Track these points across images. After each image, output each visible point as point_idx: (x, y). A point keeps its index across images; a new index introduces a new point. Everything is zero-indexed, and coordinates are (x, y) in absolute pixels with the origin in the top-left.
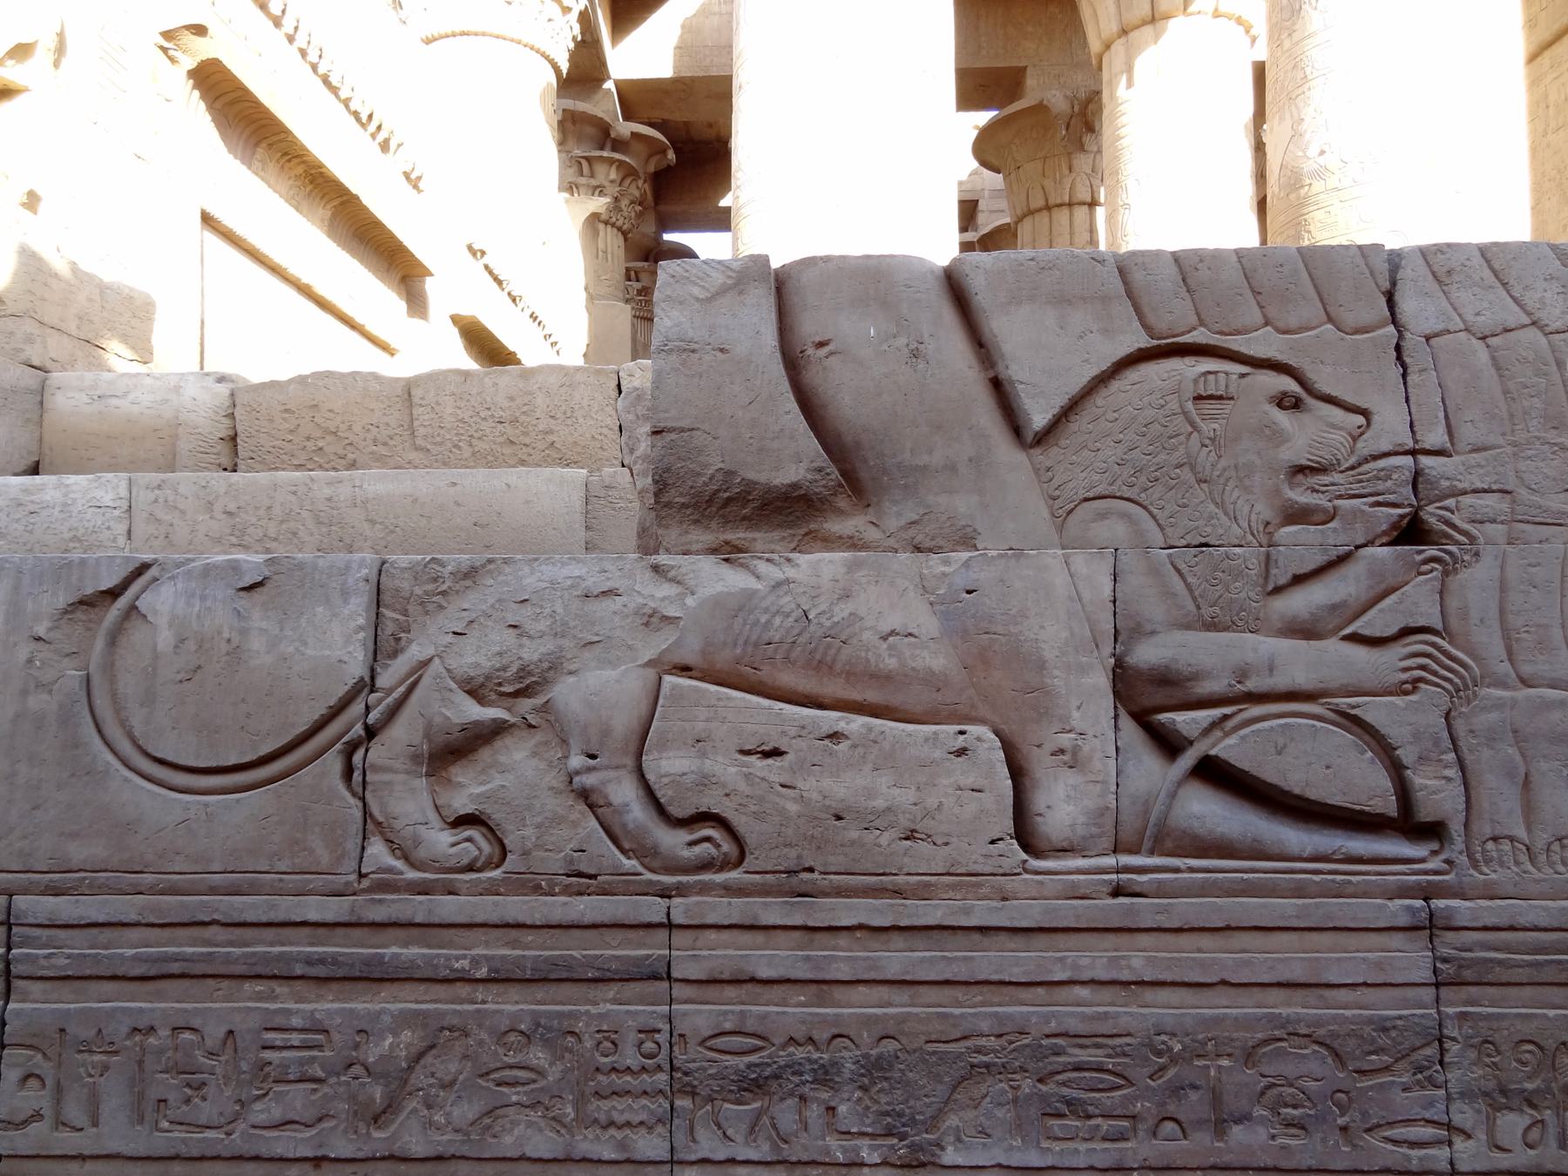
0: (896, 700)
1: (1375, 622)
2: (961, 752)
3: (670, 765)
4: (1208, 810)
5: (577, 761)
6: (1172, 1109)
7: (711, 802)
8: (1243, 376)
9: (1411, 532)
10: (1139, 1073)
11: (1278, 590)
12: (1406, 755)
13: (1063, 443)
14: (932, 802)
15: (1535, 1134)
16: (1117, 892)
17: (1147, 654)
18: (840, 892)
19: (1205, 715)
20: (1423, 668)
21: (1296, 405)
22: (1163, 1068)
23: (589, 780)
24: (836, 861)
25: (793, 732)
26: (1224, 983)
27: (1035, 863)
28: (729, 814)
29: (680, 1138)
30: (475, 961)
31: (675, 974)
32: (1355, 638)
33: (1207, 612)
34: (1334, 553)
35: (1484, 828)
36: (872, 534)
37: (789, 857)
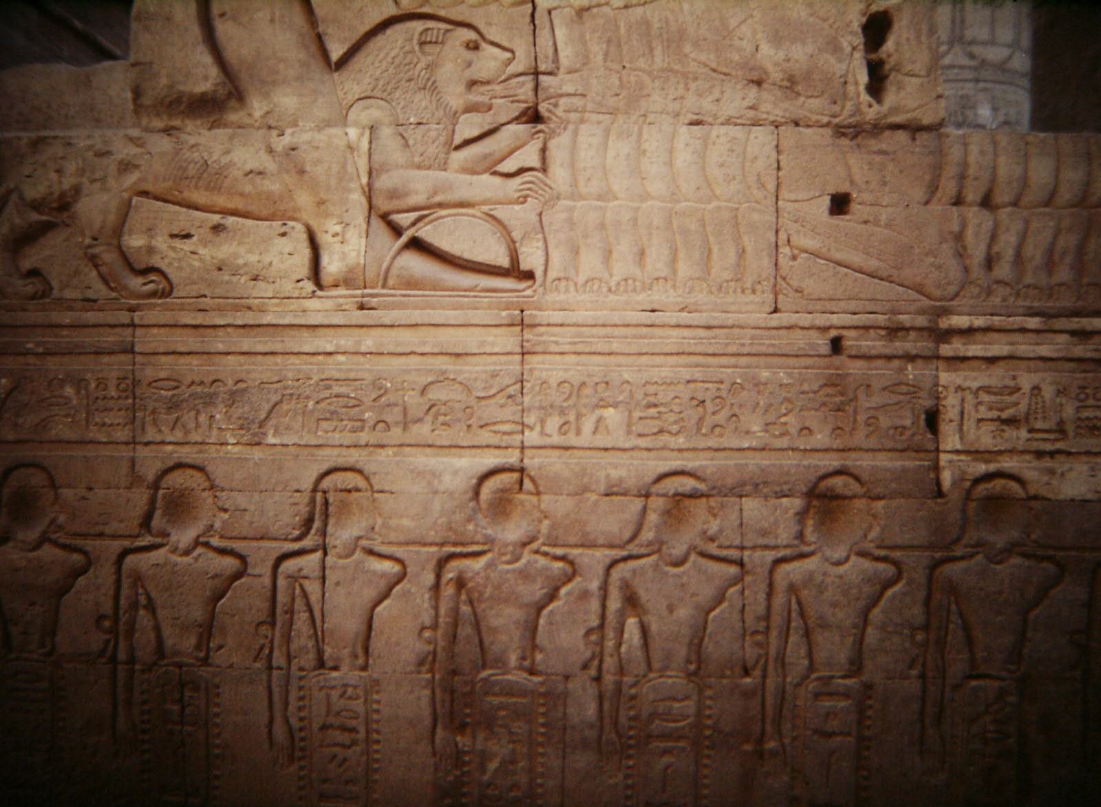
0: (253, 208)
1: (509, 166)
2: (284, 234)
3: (135, 242)
4: (415, 264)
5: (88, 241)
6: (384, 417)
7: (156, 261)
8: (448, 31)
9: (533, 117)
10: (367, 401)
11: (458, 148)
12: (516, 235)
13: (351, 68)
14: (267, 259)
15: (566, 427)
16: (362, 307)
17: (384, 182)
18: (219, 309)
19: (413, 216)
20: (529, 189)
21: (476, 48)
22: (381, 396)
23: (96, 250)
24: (219, 291)
25: (198, 224)
26: (412, 353)
27: (319, 293)
28: (164, 268)
29: (139, 431)
30: (38, 344)
31: (137, 349)
32: (495, 173)
33: (417, 159)
34: (487, 128)
35: (552, 274)
36: (247, 120)
37: (194, 290)
